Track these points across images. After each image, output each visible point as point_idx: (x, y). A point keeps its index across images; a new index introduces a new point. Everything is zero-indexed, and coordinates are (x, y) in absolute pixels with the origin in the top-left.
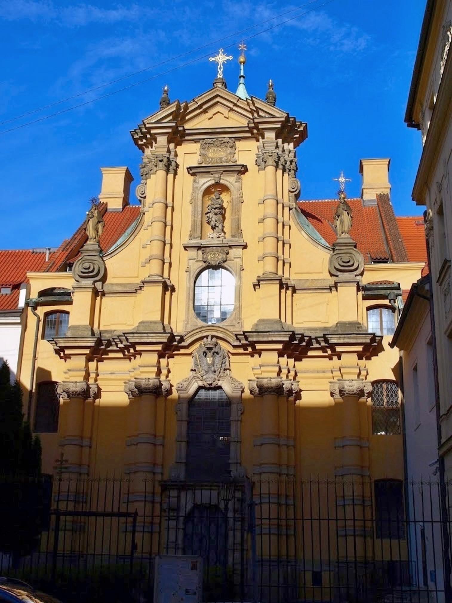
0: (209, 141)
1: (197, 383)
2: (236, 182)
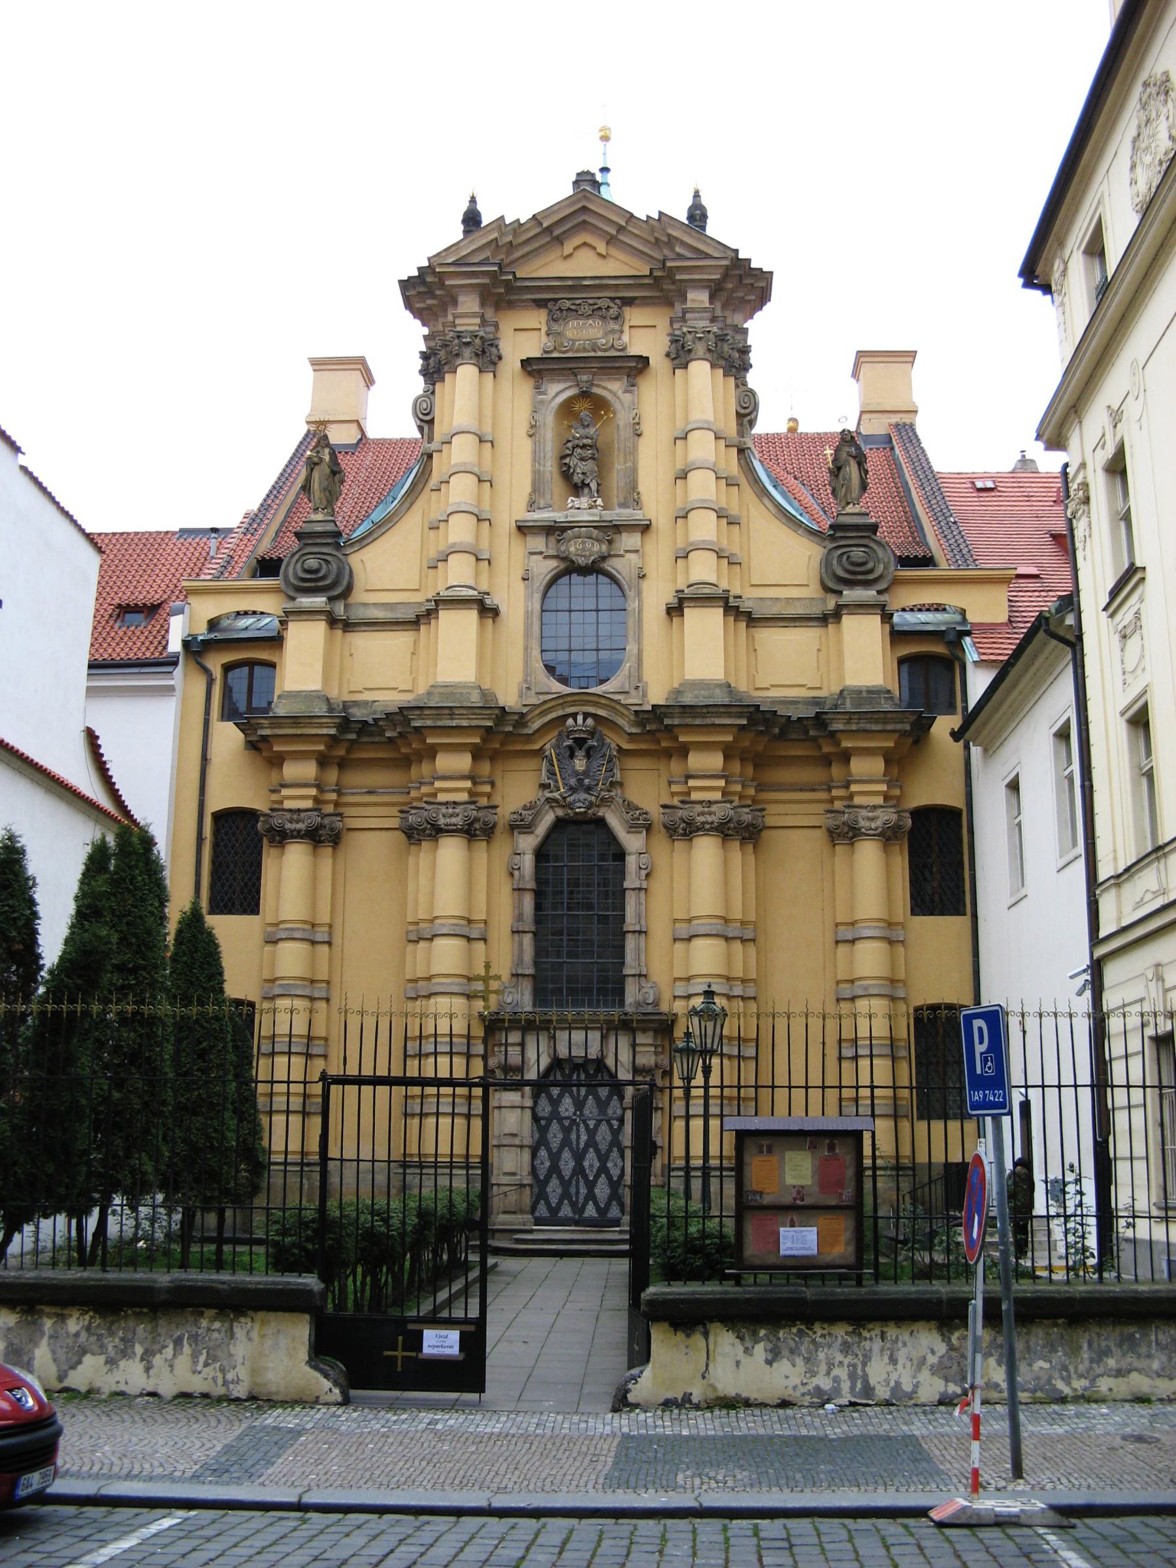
2: (626, 391)
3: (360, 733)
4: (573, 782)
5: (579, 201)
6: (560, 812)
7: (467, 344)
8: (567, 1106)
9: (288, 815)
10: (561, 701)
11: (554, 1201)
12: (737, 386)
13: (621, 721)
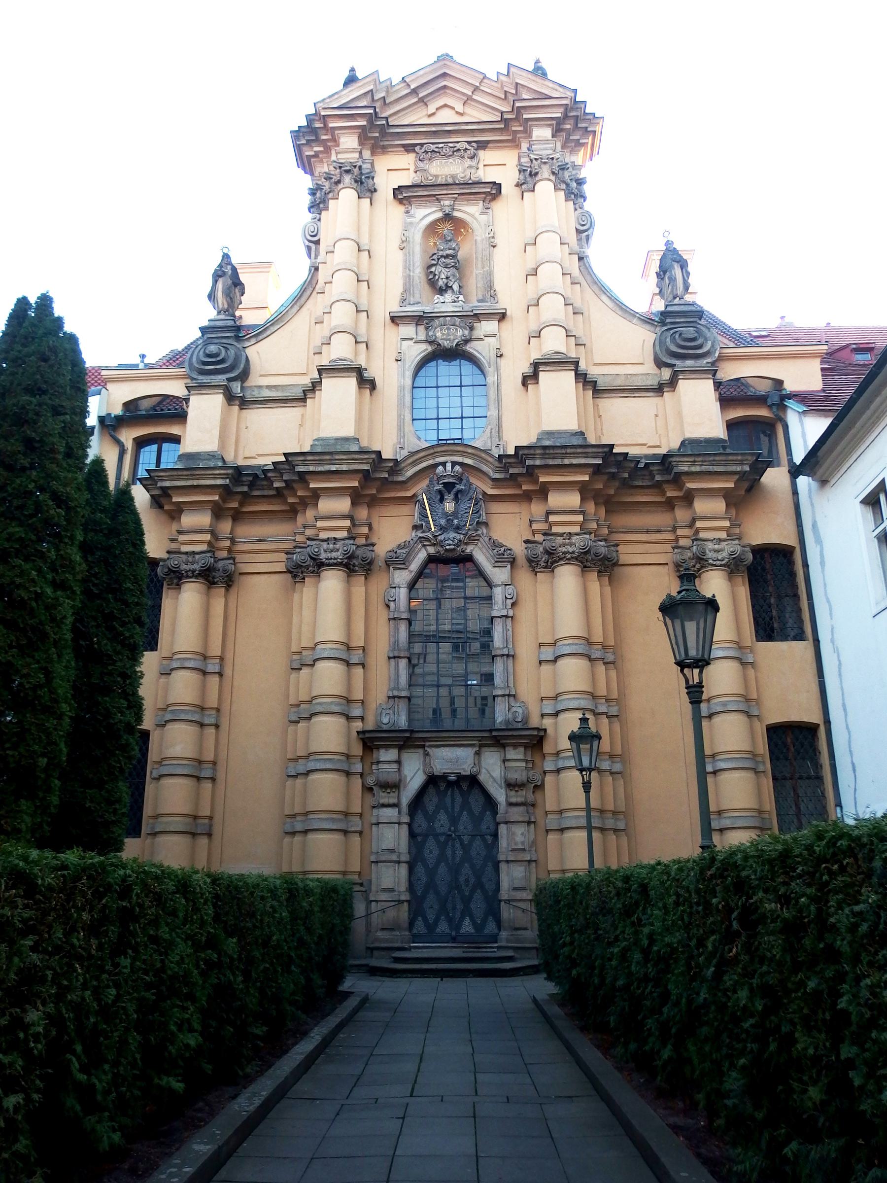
0: (433, 147)
1: (426, 550)
2: (482, 213)
3: (252, 485)
4: (443, 522)
5: (441, 68)
6: (432, 550)
7: (348, 172)
8: (442, 822)
9: (184, 557)
10: (432, 451)
11: (431, 917)
12: (576, 210)
13: (485, 468)
